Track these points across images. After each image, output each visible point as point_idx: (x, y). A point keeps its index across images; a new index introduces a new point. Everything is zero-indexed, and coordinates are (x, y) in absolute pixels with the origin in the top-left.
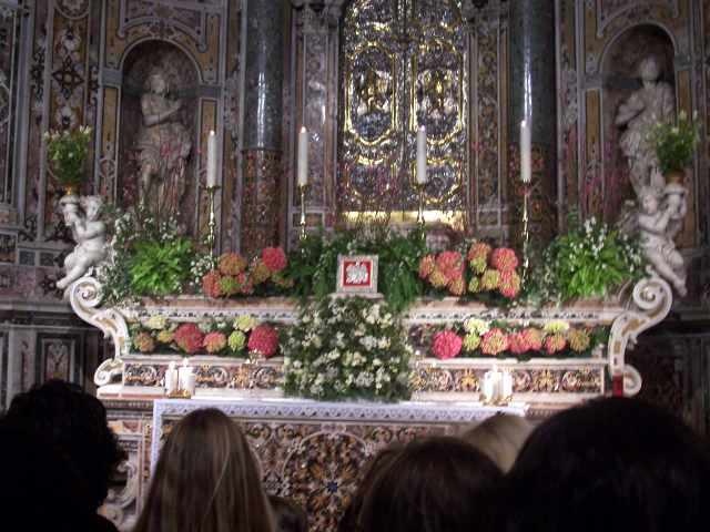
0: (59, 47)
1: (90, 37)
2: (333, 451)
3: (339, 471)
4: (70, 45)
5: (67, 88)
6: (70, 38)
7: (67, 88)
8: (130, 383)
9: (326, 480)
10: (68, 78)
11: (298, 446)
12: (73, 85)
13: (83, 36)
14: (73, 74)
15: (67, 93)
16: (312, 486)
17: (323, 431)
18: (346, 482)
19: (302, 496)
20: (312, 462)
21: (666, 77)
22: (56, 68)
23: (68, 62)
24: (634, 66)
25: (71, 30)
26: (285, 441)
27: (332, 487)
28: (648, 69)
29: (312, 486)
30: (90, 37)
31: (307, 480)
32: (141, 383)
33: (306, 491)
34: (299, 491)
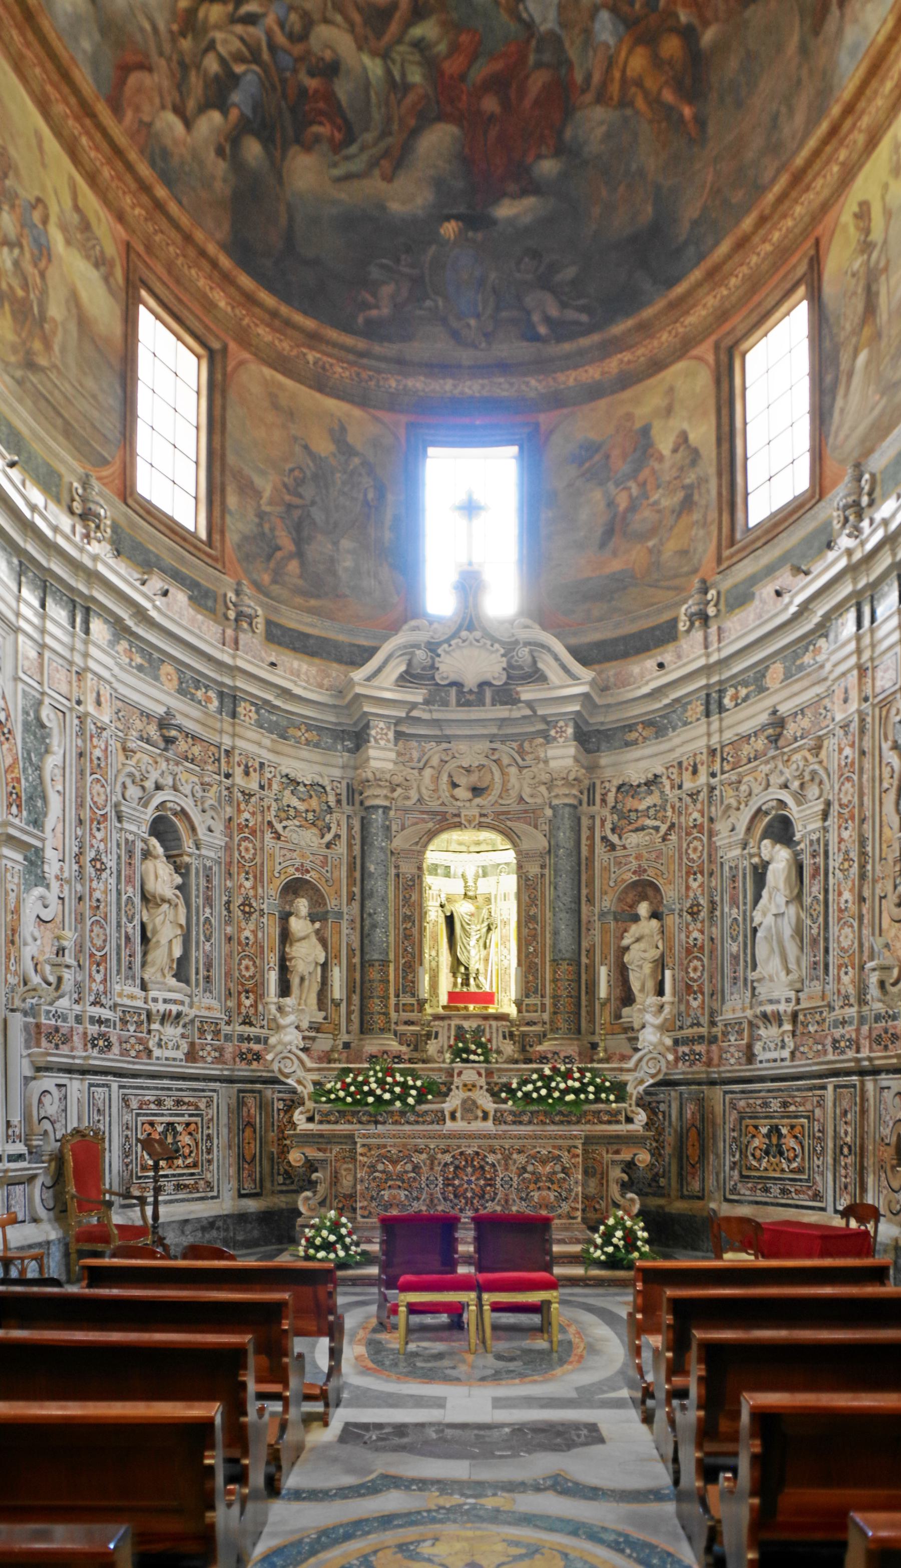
0: (241, 886)
1: (258, 879)
2: (469, 1160)
3: (474, 1172)
4: (248, 884)
5: (248, 915)
6: (247, 879)
7: (248, 915)
8: (321, 1122)
9: (465, 1178)
10: (247, 909)
11: (448, 1158)
12: (250, 913)
13: (255, 877)
14: (250, 906)
15: (247, 920)
16: (457, 1182)
17: (463, 1149)
18: (478, 1179)
19: (450, 1188)
20: (457, 1167)
21: (655, 915)
22: (240, 902)
23: (247, 898)
24: (633, 905)
25: (247, 873)
26: (439, 1156)
27: (469, 1182)
28: (643, 909)
29: (457, 1182)
30: (258, 879)
31: (453, 1179)
32: (329, 1122)
33: (453, 1185)
34: (449, 1185)
